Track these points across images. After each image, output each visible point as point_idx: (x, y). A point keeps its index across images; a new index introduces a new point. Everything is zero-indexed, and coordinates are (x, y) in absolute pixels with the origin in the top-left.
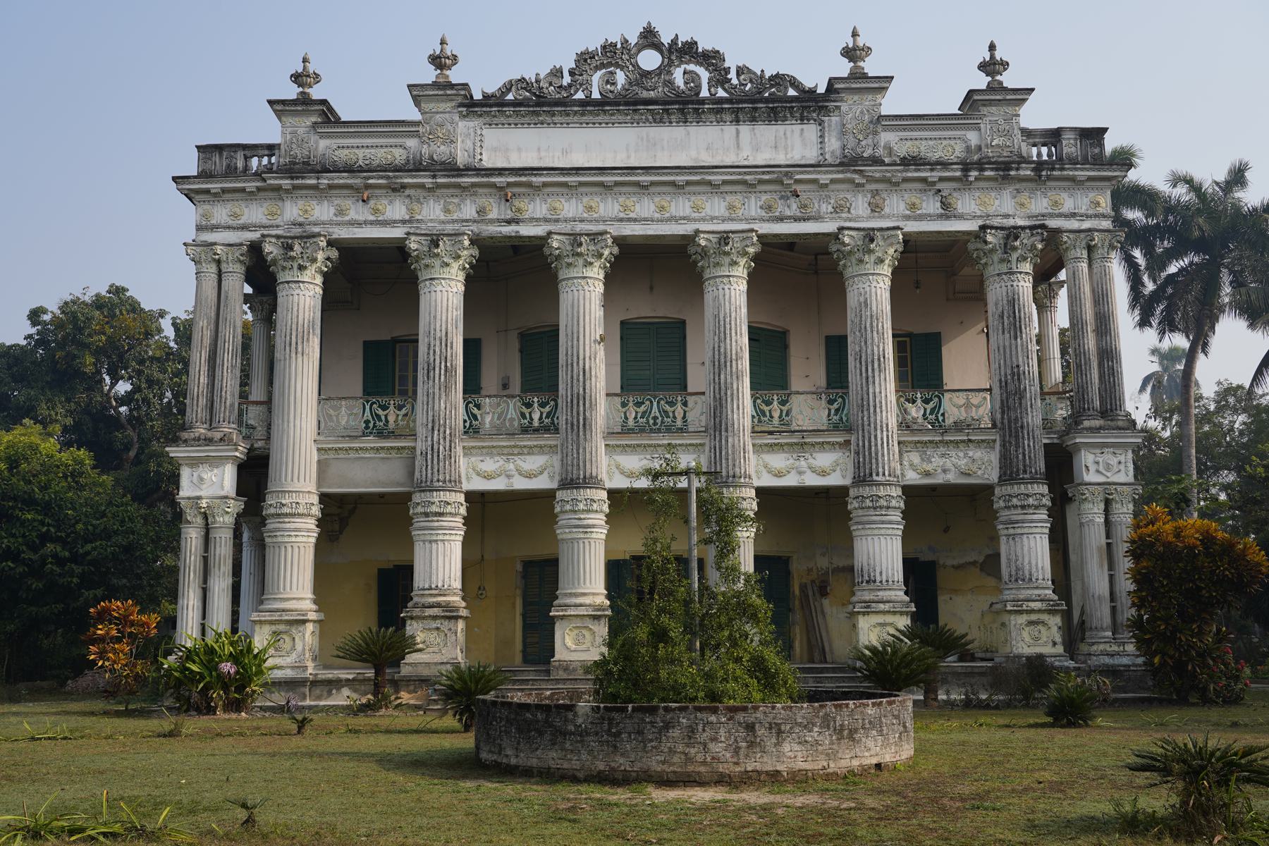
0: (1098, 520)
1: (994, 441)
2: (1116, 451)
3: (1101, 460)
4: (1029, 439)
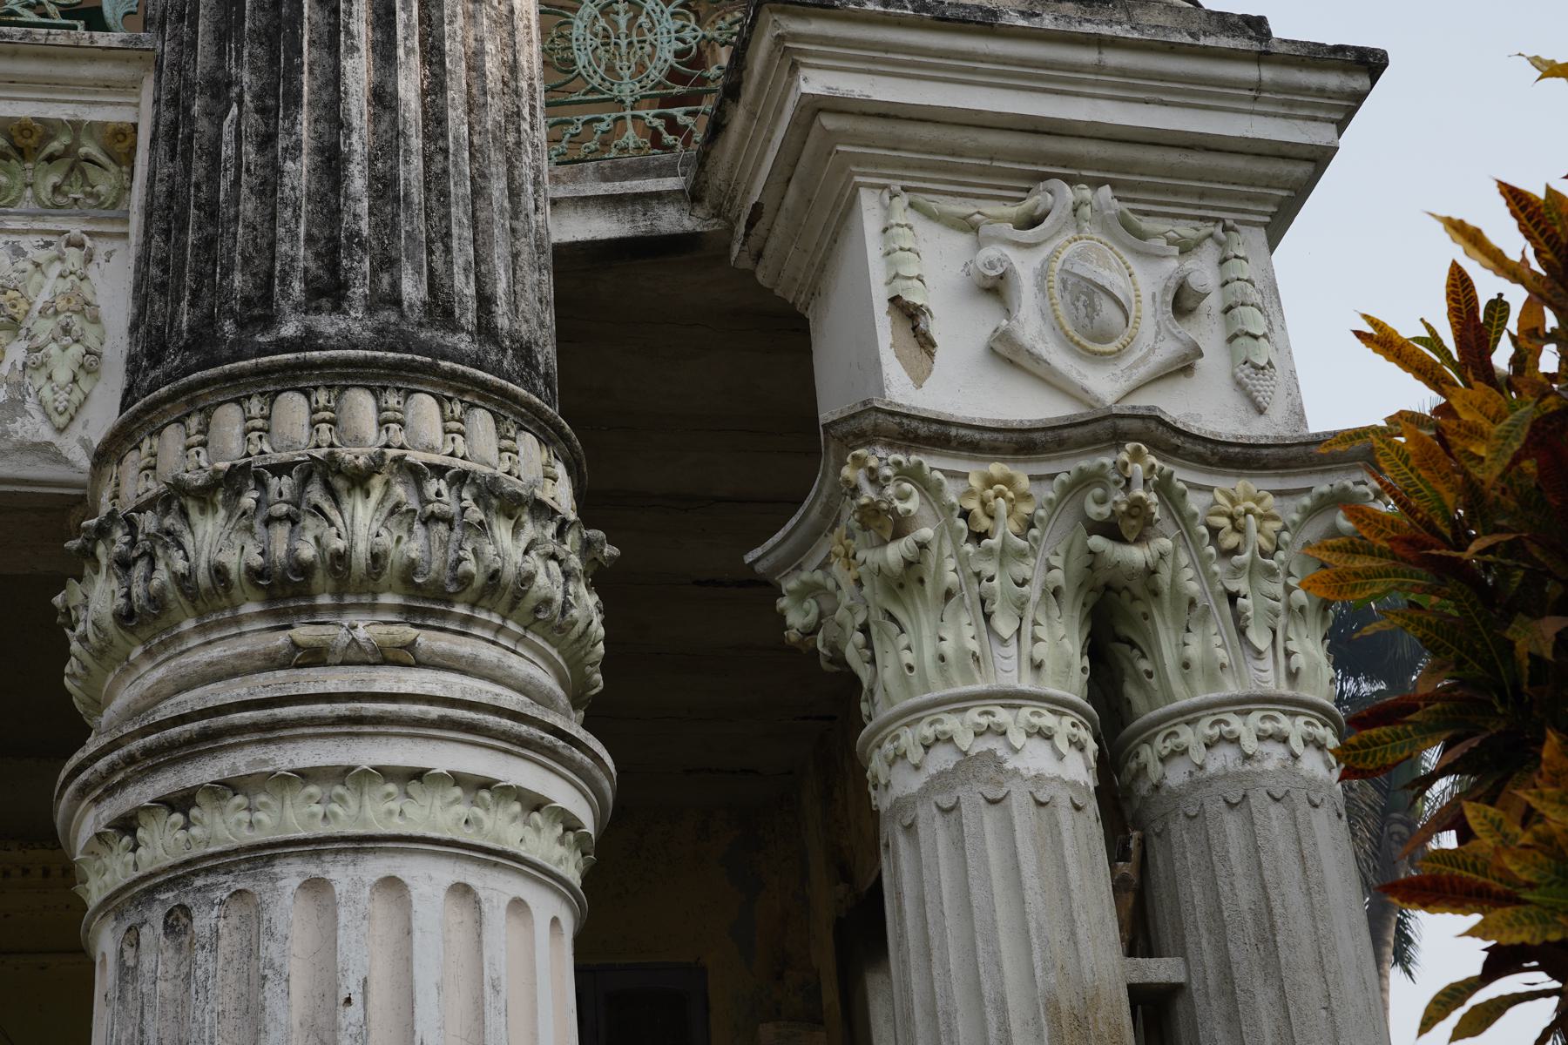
0: (1034, 759)
1: (120, 141)
2: (1146, 224)
3: (1025, 266)
4: (385, 53)
